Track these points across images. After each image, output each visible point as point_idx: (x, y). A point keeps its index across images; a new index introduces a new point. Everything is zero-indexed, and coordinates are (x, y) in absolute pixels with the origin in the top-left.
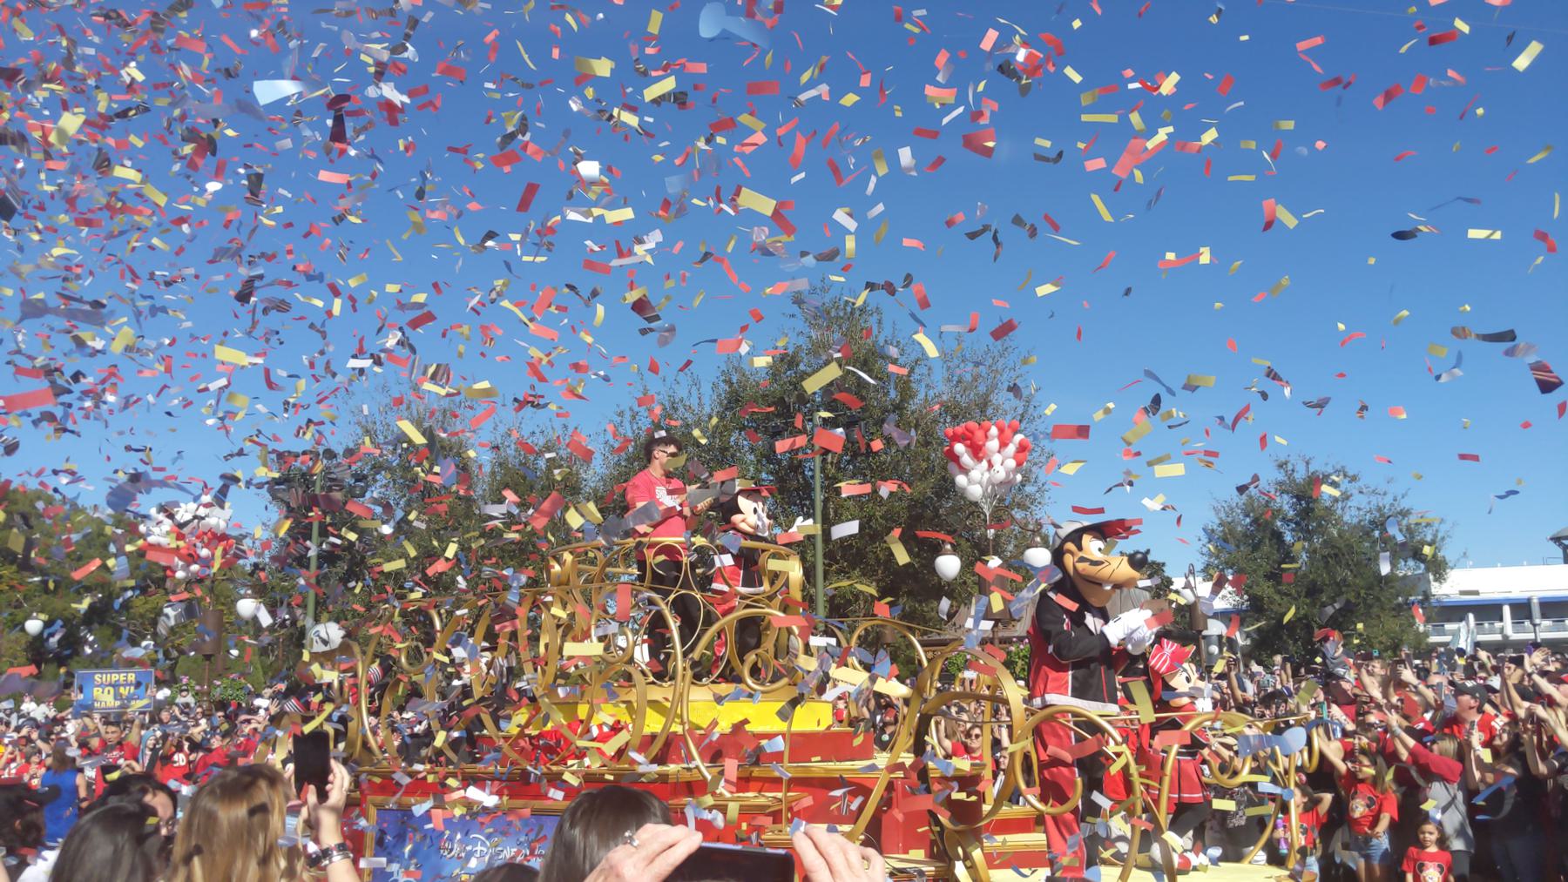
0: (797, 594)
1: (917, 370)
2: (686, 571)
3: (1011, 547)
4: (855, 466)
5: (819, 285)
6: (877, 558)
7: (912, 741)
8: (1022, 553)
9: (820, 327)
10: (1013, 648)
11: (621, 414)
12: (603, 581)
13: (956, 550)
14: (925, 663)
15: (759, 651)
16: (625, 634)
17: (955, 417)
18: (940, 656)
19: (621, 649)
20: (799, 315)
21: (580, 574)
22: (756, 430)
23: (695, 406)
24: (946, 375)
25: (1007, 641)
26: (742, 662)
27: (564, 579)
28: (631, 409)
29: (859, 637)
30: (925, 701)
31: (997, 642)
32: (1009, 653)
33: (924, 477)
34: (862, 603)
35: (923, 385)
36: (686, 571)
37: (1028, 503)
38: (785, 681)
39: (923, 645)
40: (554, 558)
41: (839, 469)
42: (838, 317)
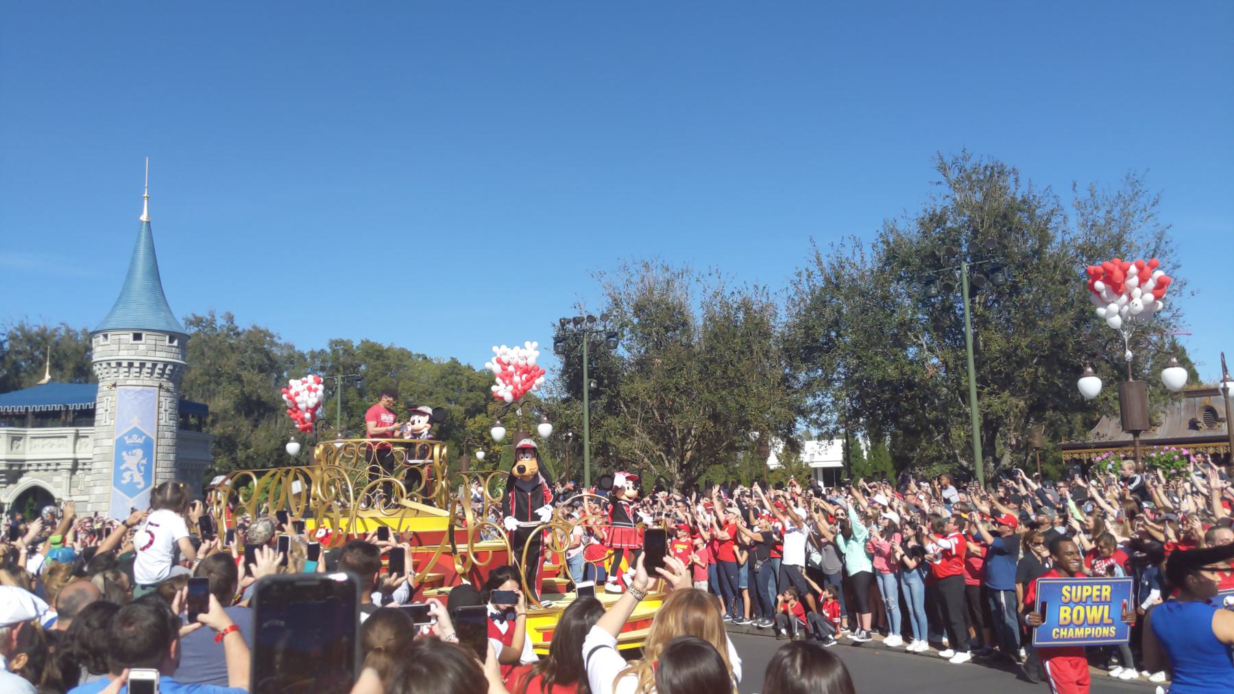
1: (1054, 219)
4: (999, 305)
6: (1024, 381)
8: (1161, 371)
10: (1154, 455)
11: (799, 274)
13: (1096, 372)
17: (1090, 258)
20: (945, 182)
22: (912, 279)
23: (858, 263)
24: (1081, 220)
28: (807, 270)
32: (1150, 459)
33: (1063, 310)
34: (1012, 418)
35: (1060, 232)
37: (1163, 327)
41: (986, 307)
42: (979, 181)
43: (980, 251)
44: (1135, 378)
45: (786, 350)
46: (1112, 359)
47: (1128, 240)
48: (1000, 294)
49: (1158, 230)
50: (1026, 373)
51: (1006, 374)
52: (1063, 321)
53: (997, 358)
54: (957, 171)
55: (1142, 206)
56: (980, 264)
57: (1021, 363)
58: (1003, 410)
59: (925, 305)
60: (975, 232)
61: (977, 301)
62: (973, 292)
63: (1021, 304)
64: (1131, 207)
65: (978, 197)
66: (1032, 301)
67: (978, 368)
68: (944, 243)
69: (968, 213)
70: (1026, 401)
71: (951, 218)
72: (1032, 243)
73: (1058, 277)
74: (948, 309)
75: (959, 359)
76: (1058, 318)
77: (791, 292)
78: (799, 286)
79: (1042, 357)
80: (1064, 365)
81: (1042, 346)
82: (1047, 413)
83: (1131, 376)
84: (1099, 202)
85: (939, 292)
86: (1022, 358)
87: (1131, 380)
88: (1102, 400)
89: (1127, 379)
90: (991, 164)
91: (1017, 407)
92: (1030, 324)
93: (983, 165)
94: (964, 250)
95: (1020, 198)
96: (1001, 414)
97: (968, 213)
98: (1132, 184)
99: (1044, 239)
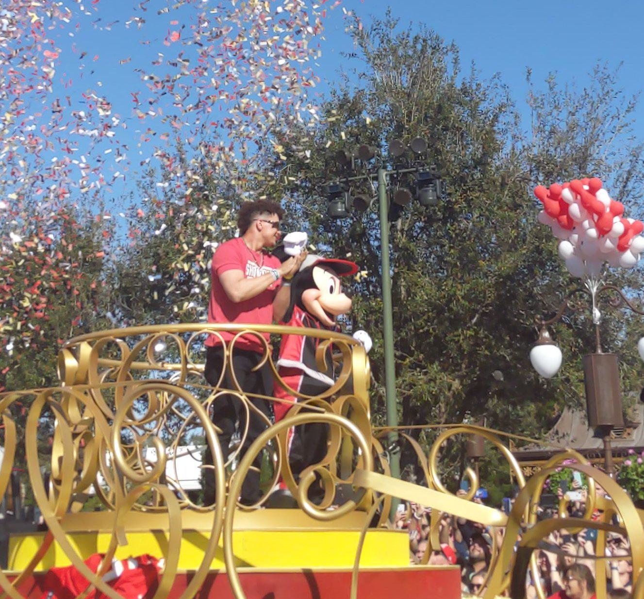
0: (362, 395)
1: (501, 118)
2: (228, 366)
3: (622, 335)
4: (429, 236)
5: (384, 19)
6: (460, 348)
7: (508, 581)
8: (636, 342)
9: (385, 68)
10: (629, 463)
12: (128, 378)
13: (555, 339)
14: (522, 482)
15: (319, 467)
16: (153, 445)
17: (548, 175)
18: (541, 473)
19: (150, 464)
20: (361, 55)
21: (100, 369)
22: (311, 190)
25: (622, 453)
26: (298, 480)
27: (81, 377)
29: (441, 449)
30: (524, 530)
31: (609, 454)
32: (625, 469)
33: (513, 247)
34: (443, 405)
35: (509, 135)
36: (228, 366)
38: (351, 504)
39: (520, 458)
40: (69, 349)
41: (411, 238)
43: (403, 155)
44: (604, 350)
45: (124, 290)
46: (576, 324)
47: (595, 155)
48: (430, 221)
49: (634, 145)
50: (463, 337)
51: (436, 337)
52: (508, 262)
53: (423, 313)
54: (377, 40)
55: (614, 112)
56: (404, 173)
57: (457, 322)
58: (430, 393)
59: (327, 229)
60: (400, 128)
61: (399, 227)
62: (393, 215)
63: (457, 235)
64: (600, 111)
65: (405, 81)
66: (472, 230)
67: (397, 328)
68: (357, 141)
69: (391, 101)
70: (461, 378)
71: (369, 107)
72: (474, 150)
73: (506, 199)
74: (360, 237)
75: (371, 312)
76: (505, 259)
77: (137, 201)
78: (150, 191)
79: (484, 314)
80: (513, 330)
81: (484, 297)
82: (490, 401)
83: (599, 346)
84: (561, 101)
85: (347, 210)
86: (457, 314)
87: (599, 351)
88: (562, 382)
89: (594, 350)
90: (423, 35)
91: (449, 389)
92: (469, 265)
93: (413, 35)
94: (385, 154)
95: (458, 86)
96: (427, 397)
97: (391, 101)
98: (603, 81)
99: (490, 146)
